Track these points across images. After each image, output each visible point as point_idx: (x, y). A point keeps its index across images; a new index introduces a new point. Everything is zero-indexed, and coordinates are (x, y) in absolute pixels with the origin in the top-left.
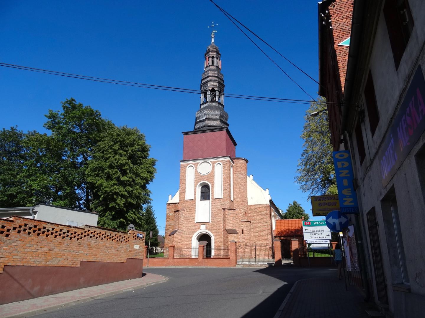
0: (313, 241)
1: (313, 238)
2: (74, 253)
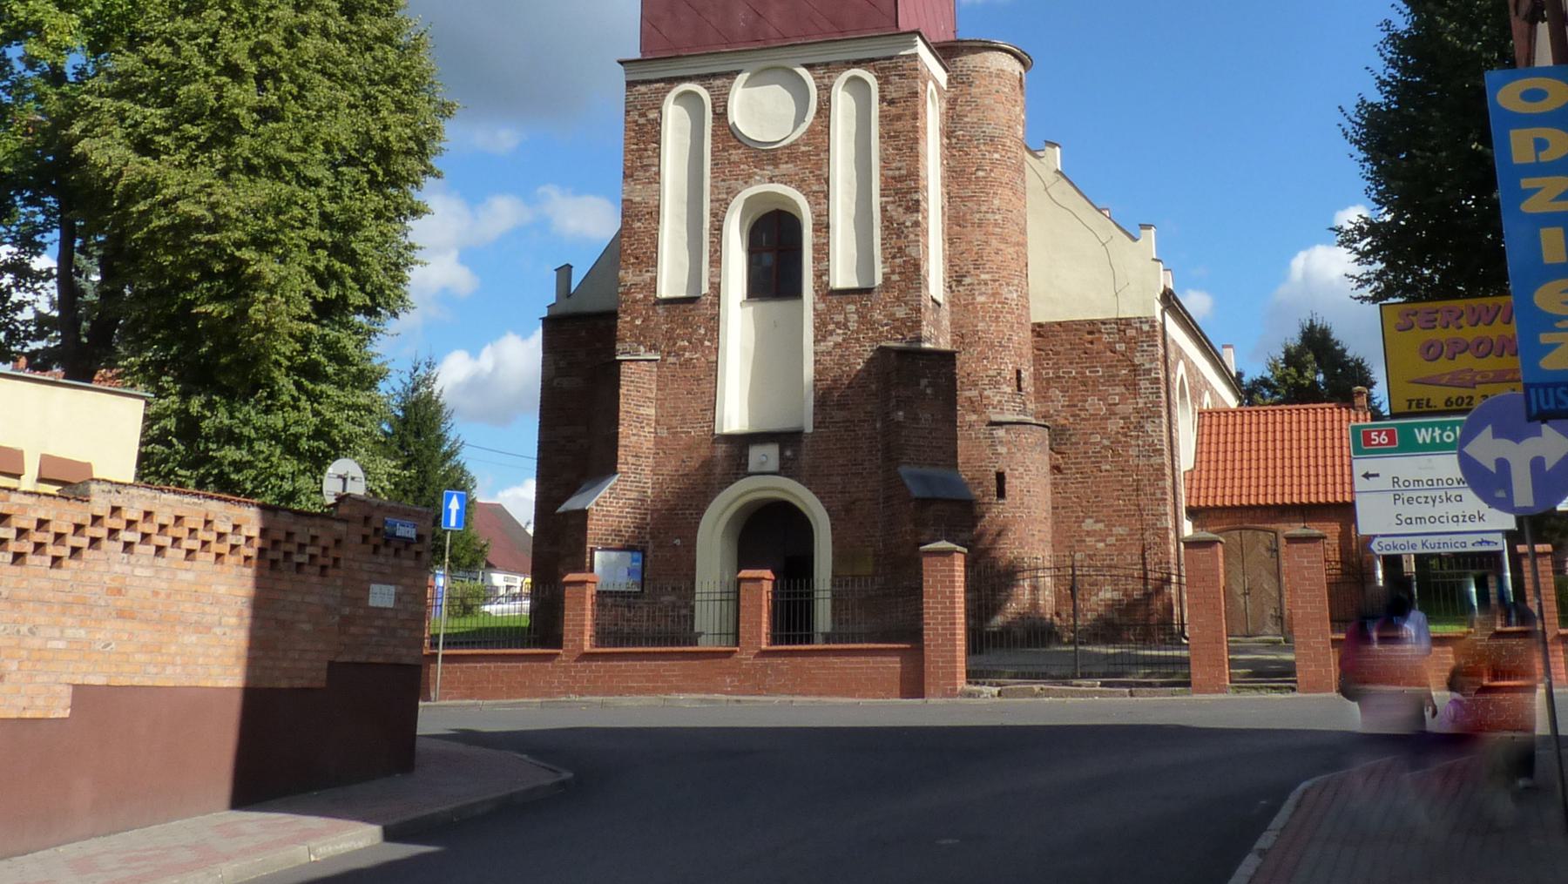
0: (1412, 540)
1: (1409, 521)
2: (35, 643)
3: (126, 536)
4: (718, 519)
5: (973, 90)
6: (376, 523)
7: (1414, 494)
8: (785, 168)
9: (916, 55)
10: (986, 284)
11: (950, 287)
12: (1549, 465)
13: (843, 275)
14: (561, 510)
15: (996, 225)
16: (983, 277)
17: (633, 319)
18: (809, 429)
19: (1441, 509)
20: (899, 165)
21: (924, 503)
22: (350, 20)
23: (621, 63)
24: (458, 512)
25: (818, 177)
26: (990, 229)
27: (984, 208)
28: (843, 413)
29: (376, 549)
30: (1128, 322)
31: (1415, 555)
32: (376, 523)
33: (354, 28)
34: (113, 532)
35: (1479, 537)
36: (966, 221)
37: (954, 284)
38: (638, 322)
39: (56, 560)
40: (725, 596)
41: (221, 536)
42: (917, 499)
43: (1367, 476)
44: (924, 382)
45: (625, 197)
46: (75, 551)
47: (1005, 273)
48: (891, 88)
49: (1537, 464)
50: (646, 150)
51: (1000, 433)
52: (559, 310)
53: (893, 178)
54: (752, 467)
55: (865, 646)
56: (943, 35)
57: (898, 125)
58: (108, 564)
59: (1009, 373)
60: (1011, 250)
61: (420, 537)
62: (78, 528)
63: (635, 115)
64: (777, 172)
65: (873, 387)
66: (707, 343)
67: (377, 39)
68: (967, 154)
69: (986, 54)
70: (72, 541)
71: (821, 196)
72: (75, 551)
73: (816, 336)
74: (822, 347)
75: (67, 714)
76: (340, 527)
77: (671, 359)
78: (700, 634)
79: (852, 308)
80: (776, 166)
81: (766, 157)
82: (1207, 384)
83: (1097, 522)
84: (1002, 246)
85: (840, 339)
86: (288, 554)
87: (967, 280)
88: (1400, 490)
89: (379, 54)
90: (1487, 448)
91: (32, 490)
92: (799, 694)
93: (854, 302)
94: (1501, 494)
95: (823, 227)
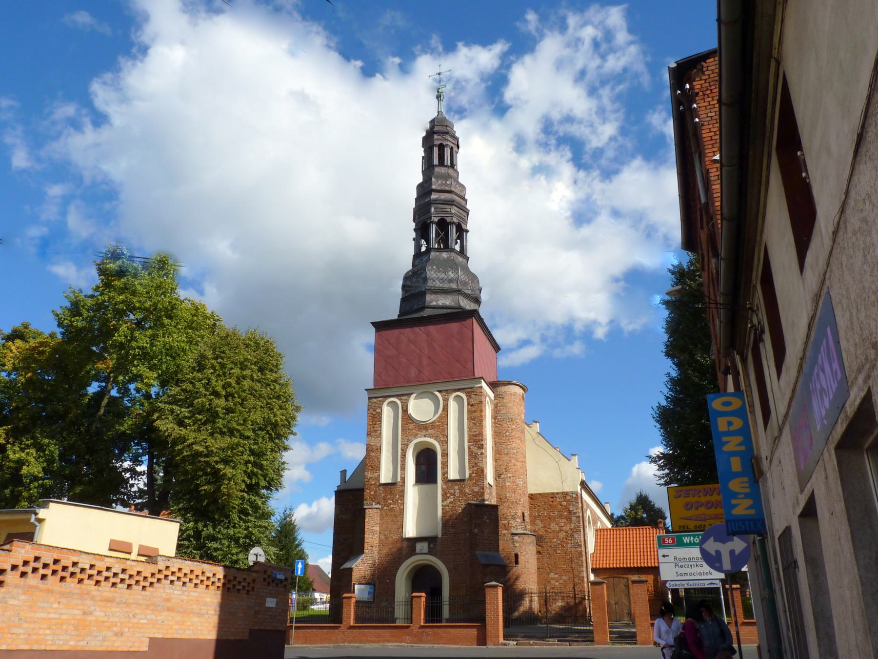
0: (683, 582)
1: (681, 575)
2: (135, 621)
3: (171, 578)
4: (404, 572)
5: (504, 400)
6: (269, 573)
7: (683, 564)
8: (430, 431)
9: (482, 387)
10: (510, 478)
11: (496, 479)
12: (737, 553)
13: (453, 474)
14: (342, 568)
15: (514, 454)
16: (509, 475)
17: (370, 492)
18: (440, 536)
19: (694, 570)
20: (475, 430)
21: (486, 566)
22: (262, 374)
23: (366, 390)
24: (301, 569)
25: (443, 435)
26: (511, 455)
27: (509, 447)
28: (453, 530)
29: (269, 583)
30: (567, 493)
31: (684, 589)
32: (269, 573)
33: (263, 377)
34: (166, 576)
35: (710, 582)
36: (502, 452)
37: (497, 478)
38: (372, 493)
39: (144, 587)
40: (406, 603)
41: (208, 578)
42: (483, 564)
43: (664, 556)
44: (485, 517)
45: (367, 443)
46: (151, 584)
47: (517, 474)
48: (472, 400)
49: (732, 552)
50: (376, 424)
51: (516, 538)
52: (342, 488)
53: (473, 435)
54: (417, 551)
55: (463, 624)
56: (492, 379)
57: (475, 415)
58: (164, 590)
59: (520, 514)
60: (520, 464)
61: (286, 579)
62: (153, 574)
63: (371, 411)
64: (427, 433)
65: (465, 519)
66: (399, 501)
67: (272, 381)
68: (502, 426)
69: (509, 386)
70: (150, 580)
71: (445, 442)
72: (151, 584)
73: (442, 499)
74: (445, 503)
75: (146, 649)
76: (255, 575)
77: (385, 508)
78: (397, 618)
79: (457, 487)
80: (427, 430)
81: (423, 427)
82: (599, 518)
83: (556, 574)
84: (516, 463)
85: (452, 500)
86: (234, 586)
87: (503, 476)
88: (677, 562)
89: (272, 387)
90: (712, 546)
91: (135, 559)
92: (437, 643)
93: (458, 485)
94: (718, 565)
95: (445, 455)
